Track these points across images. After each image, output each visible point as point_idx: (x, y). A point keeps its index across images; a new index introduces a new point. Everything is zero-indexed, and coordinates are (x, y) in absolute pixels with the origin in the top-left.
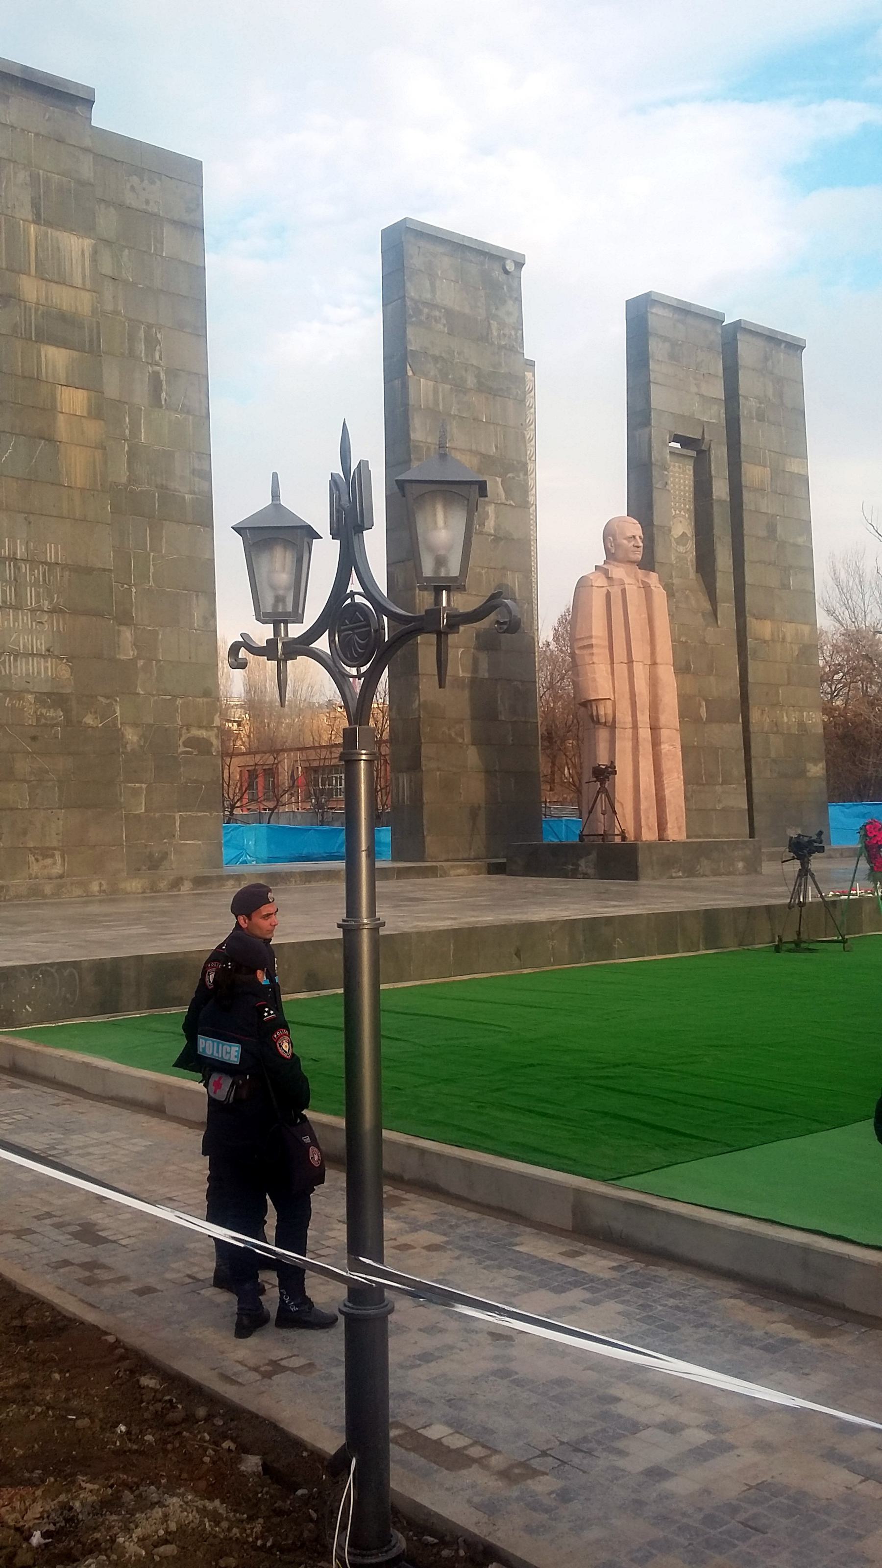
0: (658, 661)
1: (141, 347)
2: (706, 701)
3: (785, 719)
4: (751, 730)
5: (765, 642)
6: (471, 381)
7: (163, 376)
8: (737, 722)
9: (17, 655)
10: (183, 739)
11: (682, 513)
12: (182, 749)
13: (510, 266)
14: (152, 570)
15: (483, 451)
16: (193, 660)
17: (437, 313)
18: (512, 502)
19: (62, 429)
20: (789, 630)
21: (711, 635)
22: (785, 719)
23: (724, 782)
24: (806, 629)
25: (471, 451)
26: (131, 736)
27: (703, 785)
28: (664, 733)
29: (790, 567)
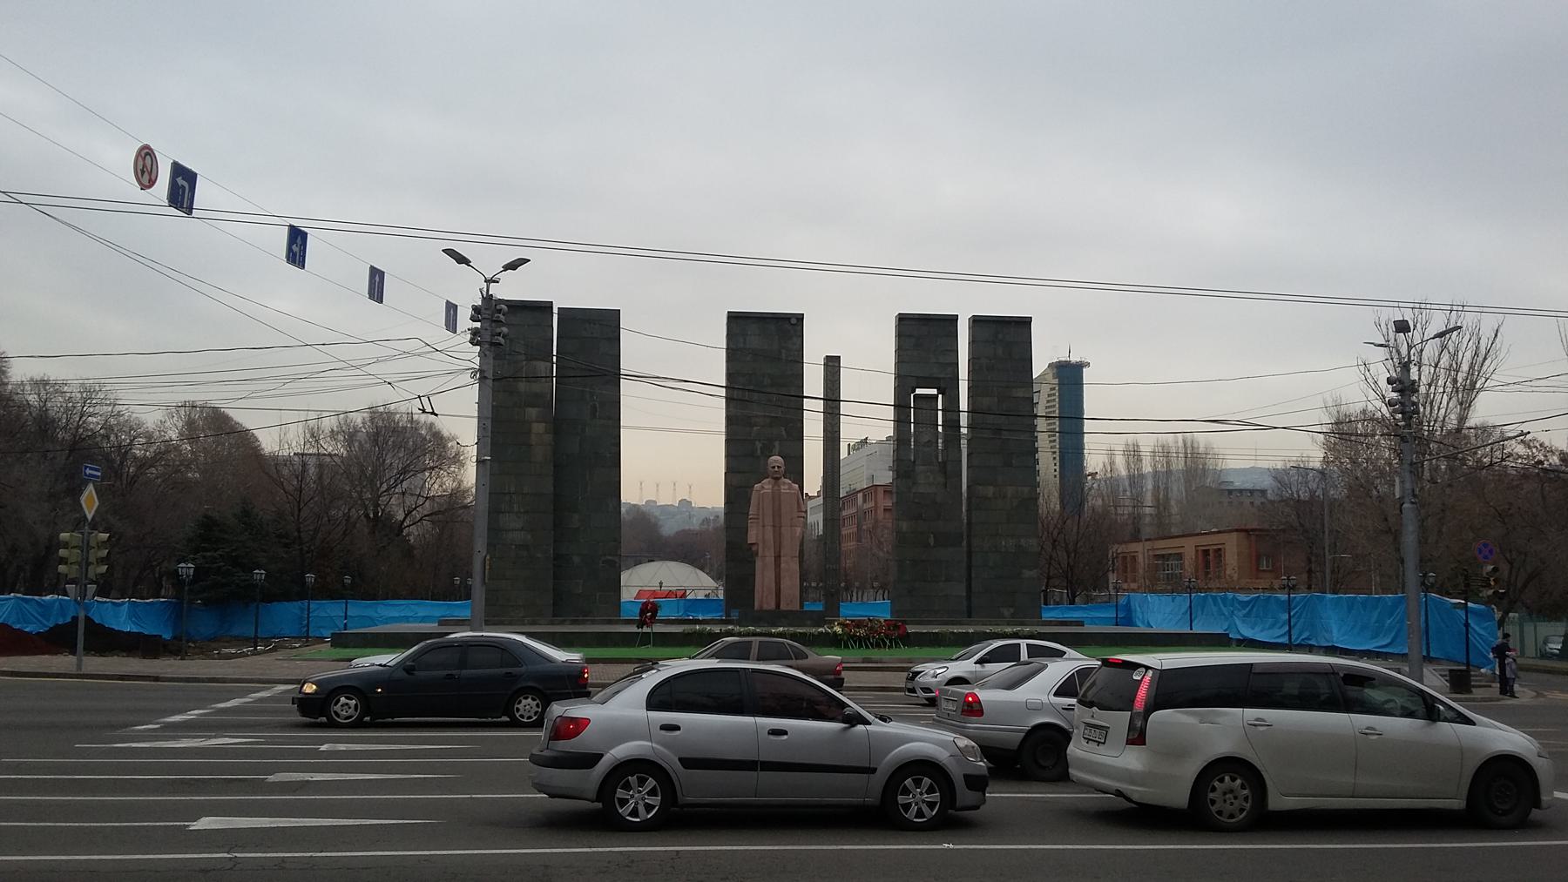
20: (1010, 491)
24: (1026, 490)
26: (576, 559)
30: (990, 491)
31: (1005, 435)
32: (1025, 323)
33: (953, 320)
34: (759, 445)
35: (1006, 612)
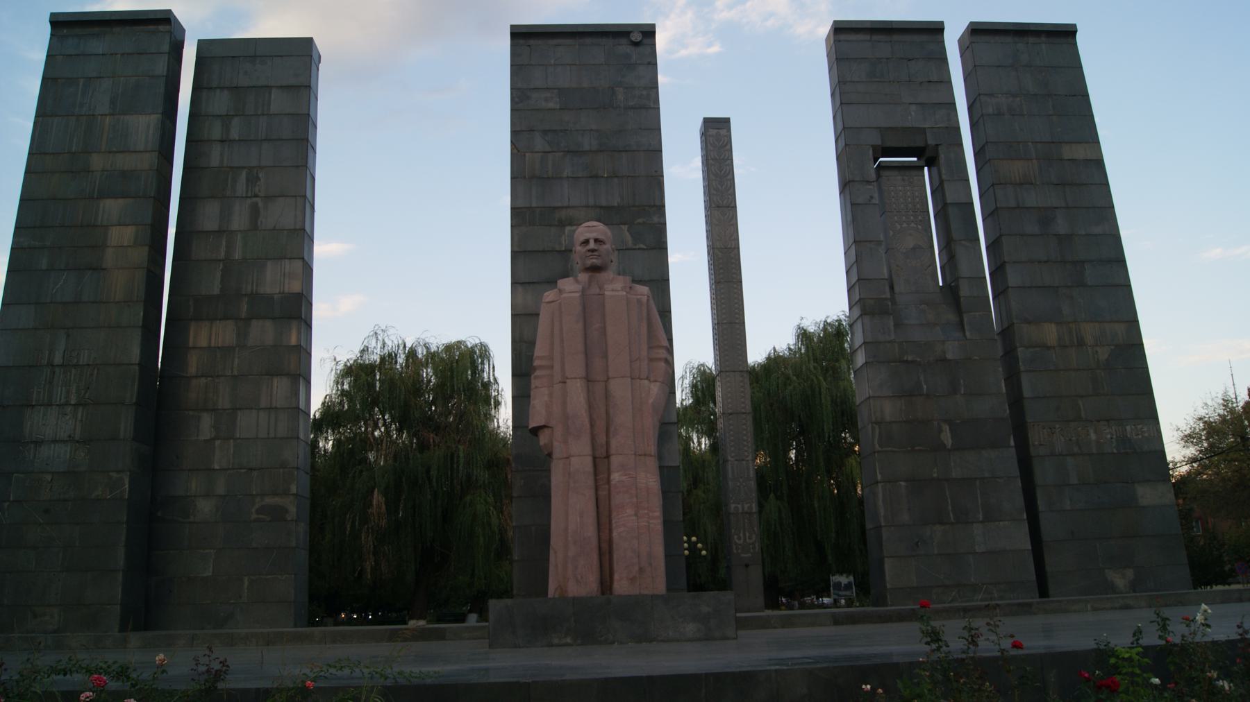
0: (610, 375)
1: (241, 187)
3: (1093, 436)
4: (1033, 452)
5: (1049, 348)
6: (588, 143)
7: (260, 204)
9: (39, 443)
10: (257, 506)
11: (913, 225)
12: (254, 516)
13: (636, 37)
14: (236, 361)
15: (604, 203)
16: (272, 435)
18: (642, 246)
20: (1089, 331)
21: (952, 351)
22: (1093, 436)
25: (587, 207)
26: (205, 507)
28: (615, 460)
29: (1083, 262)
30: (1050, 333)
31: (1061, 226)
32: (1066, 34)
33: (936, 29)
35: (1120, 580)
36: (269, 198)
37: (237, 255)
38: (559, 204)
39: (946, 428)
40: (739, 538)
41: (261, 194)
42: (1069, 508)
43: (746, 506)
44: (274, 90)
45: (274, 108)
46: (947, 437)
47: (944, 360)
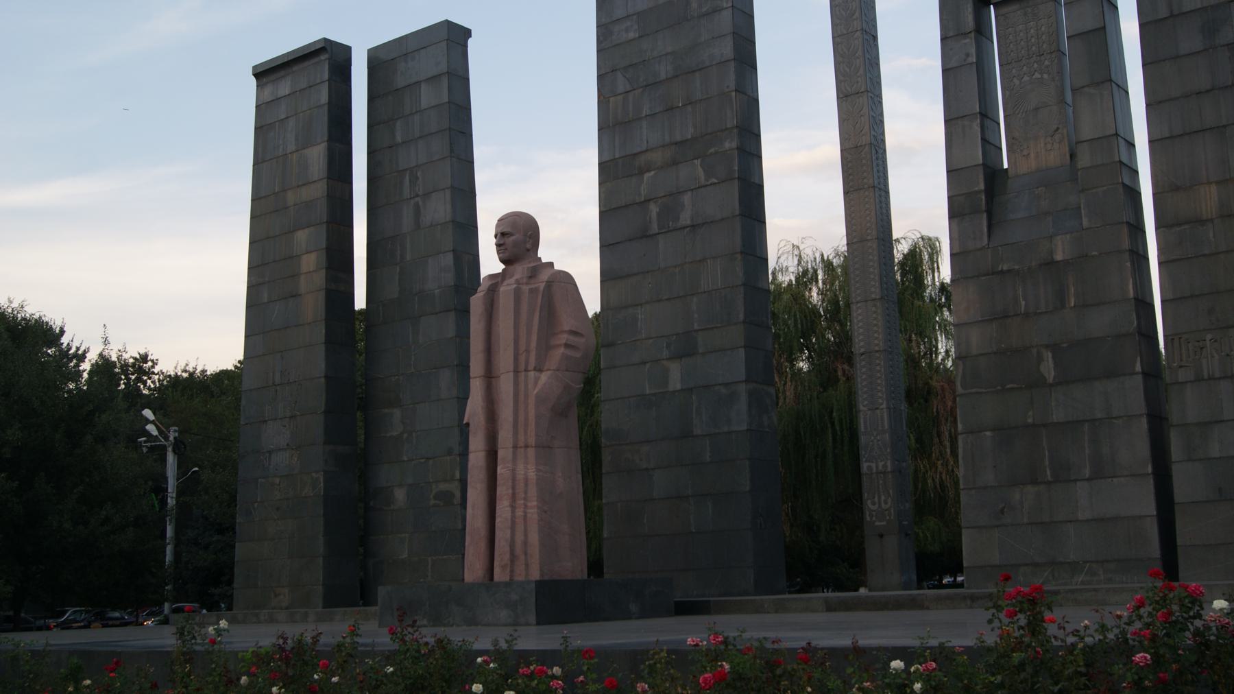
1: (406, 192)
2: (1054, 348)
5: (1200, 222)
8: (1134, 373)
9: (270, 452)
12: (432, 502)
15: (678, 138)
17: (629, 23)
19: (303, 285)
23: (1098, 474)
26: (400, 495)
27: (1049, 483)
28: (501, 453)
34: (654, 209)
36: (427, 195)
37: (408, 257)
38: (639, 150)
39: (1048, 356)
40: (874, 504)
41: (420, 193)
42: (1217, 455)
43: (881, 464)
44: (423, 85)
45: (424, 103)
46: (1048, 369)
47: (1050, 264)
